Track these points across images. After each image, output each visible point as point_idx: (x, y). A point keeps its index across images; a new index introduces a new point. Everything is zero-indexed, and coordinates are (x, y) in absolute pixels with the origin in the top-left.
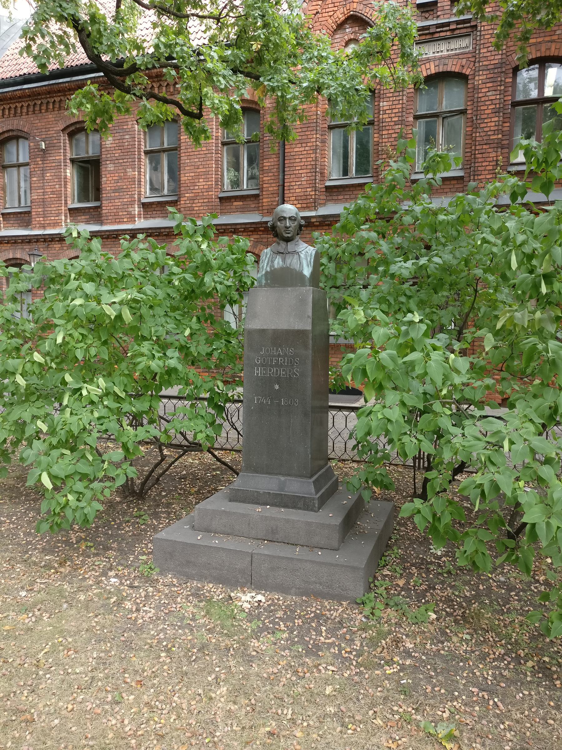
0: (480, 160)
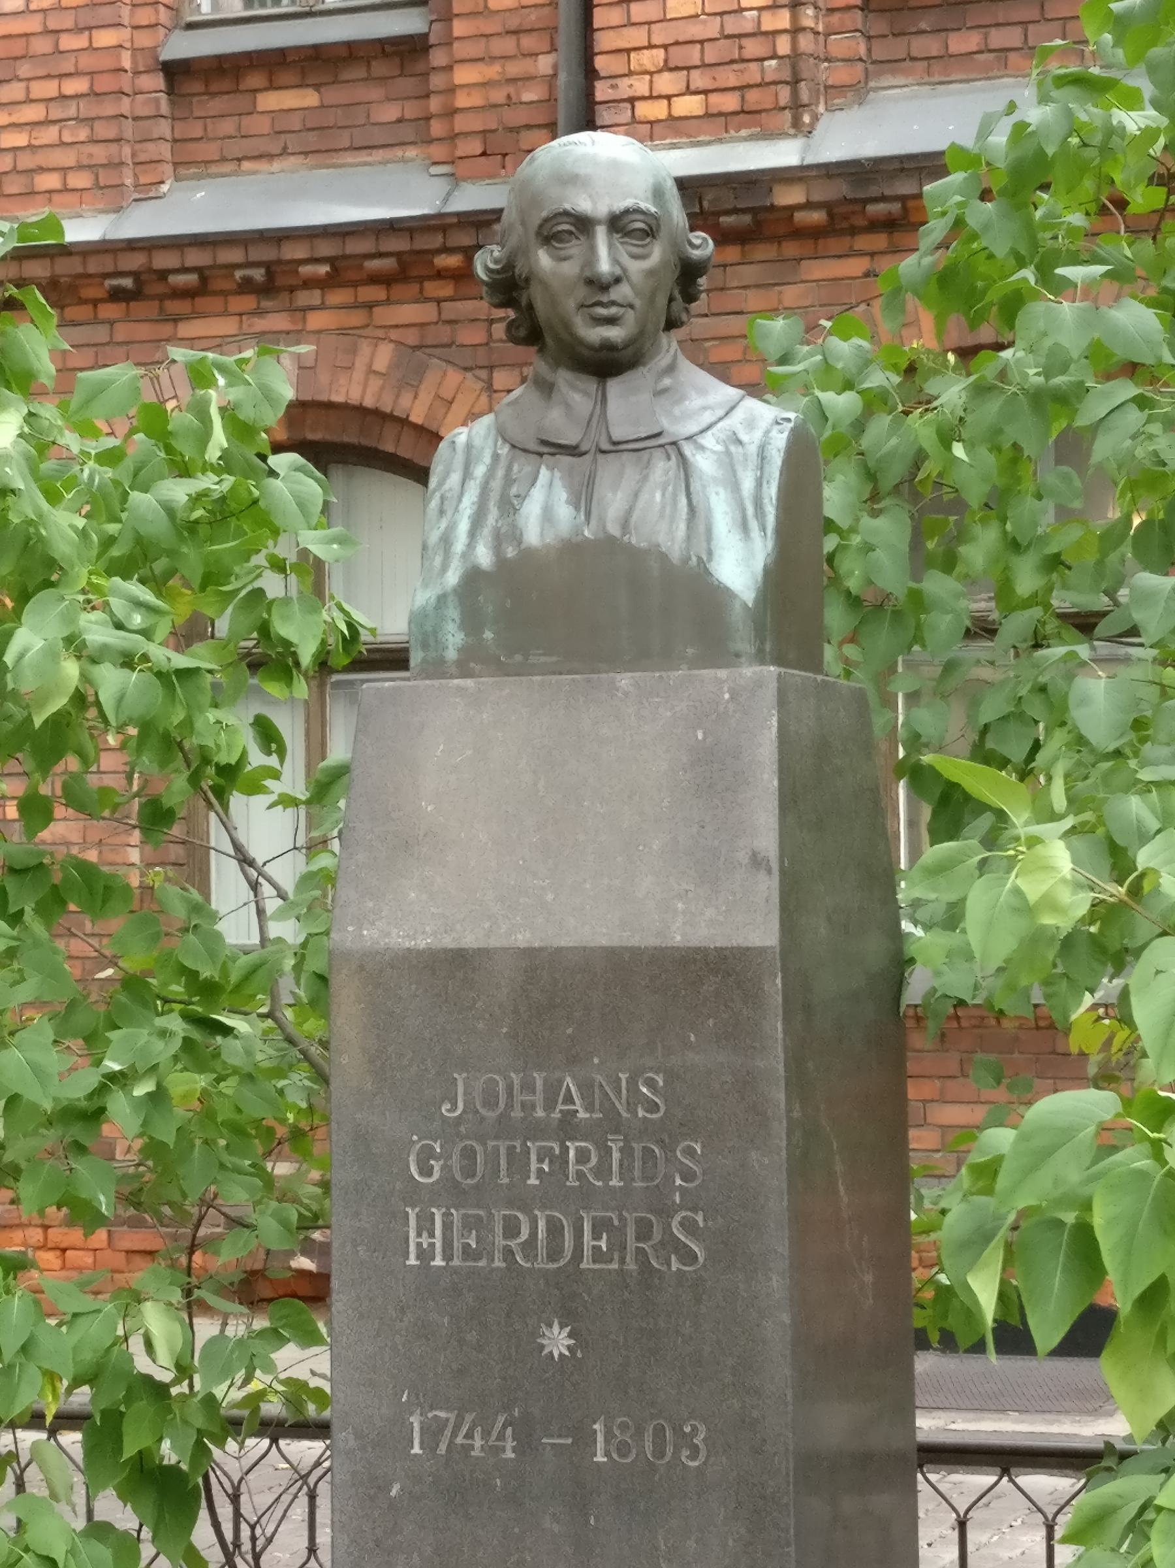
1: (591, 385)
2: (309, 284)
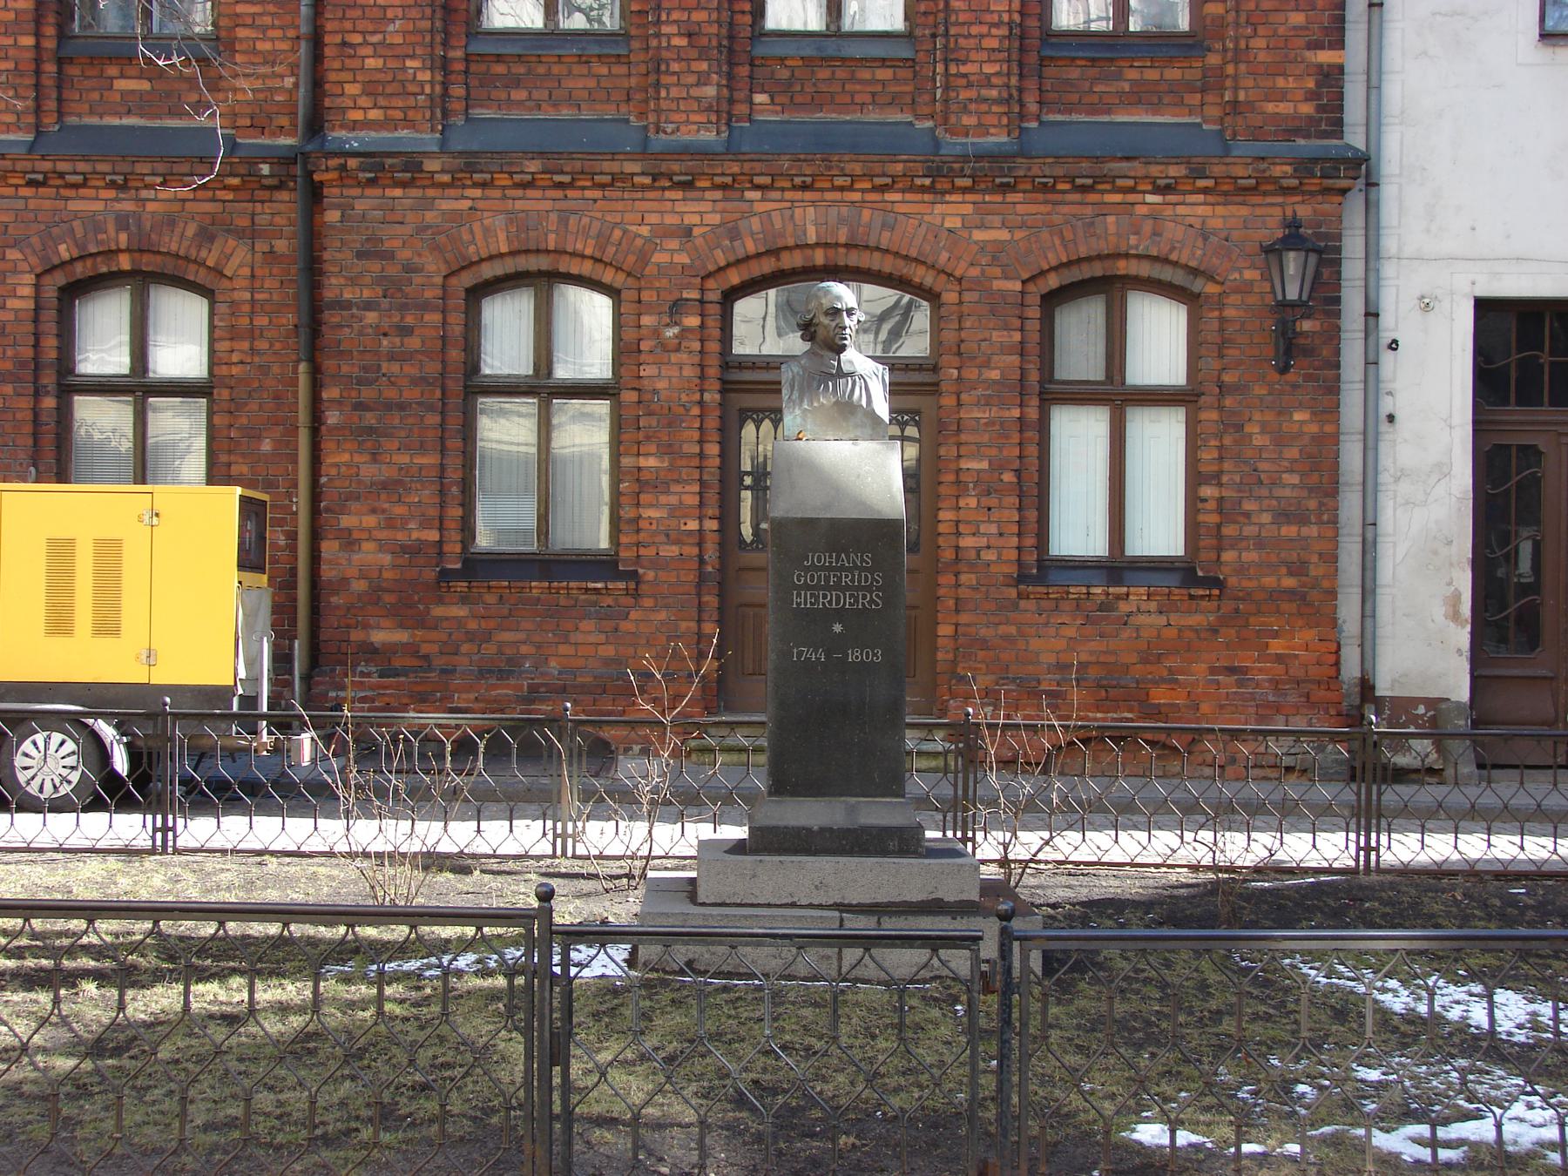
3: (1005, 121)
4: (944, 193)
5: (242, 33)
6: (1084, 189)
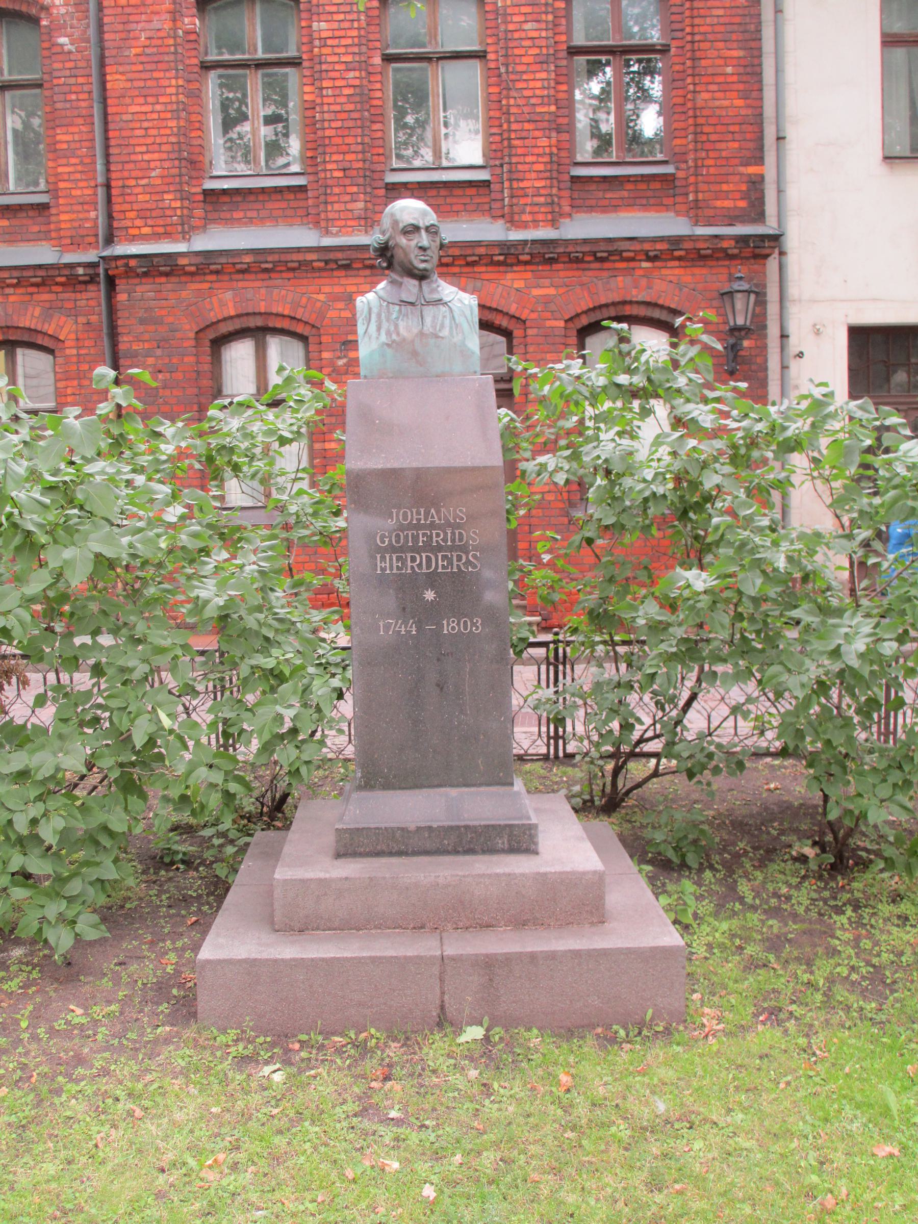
0: (520, 151)
1: (416, 282)
2: (9, 286)
3: (549, 217)
4: (512, 265)
5: (62, 185)
6: (602, 260)
